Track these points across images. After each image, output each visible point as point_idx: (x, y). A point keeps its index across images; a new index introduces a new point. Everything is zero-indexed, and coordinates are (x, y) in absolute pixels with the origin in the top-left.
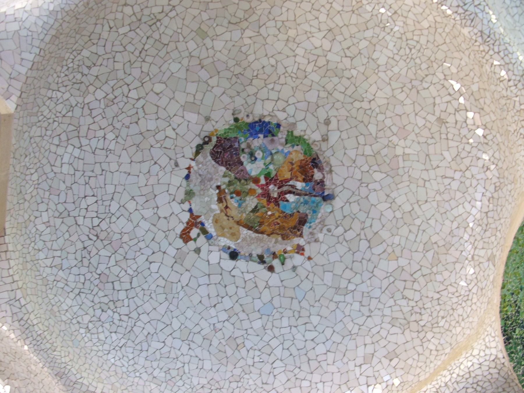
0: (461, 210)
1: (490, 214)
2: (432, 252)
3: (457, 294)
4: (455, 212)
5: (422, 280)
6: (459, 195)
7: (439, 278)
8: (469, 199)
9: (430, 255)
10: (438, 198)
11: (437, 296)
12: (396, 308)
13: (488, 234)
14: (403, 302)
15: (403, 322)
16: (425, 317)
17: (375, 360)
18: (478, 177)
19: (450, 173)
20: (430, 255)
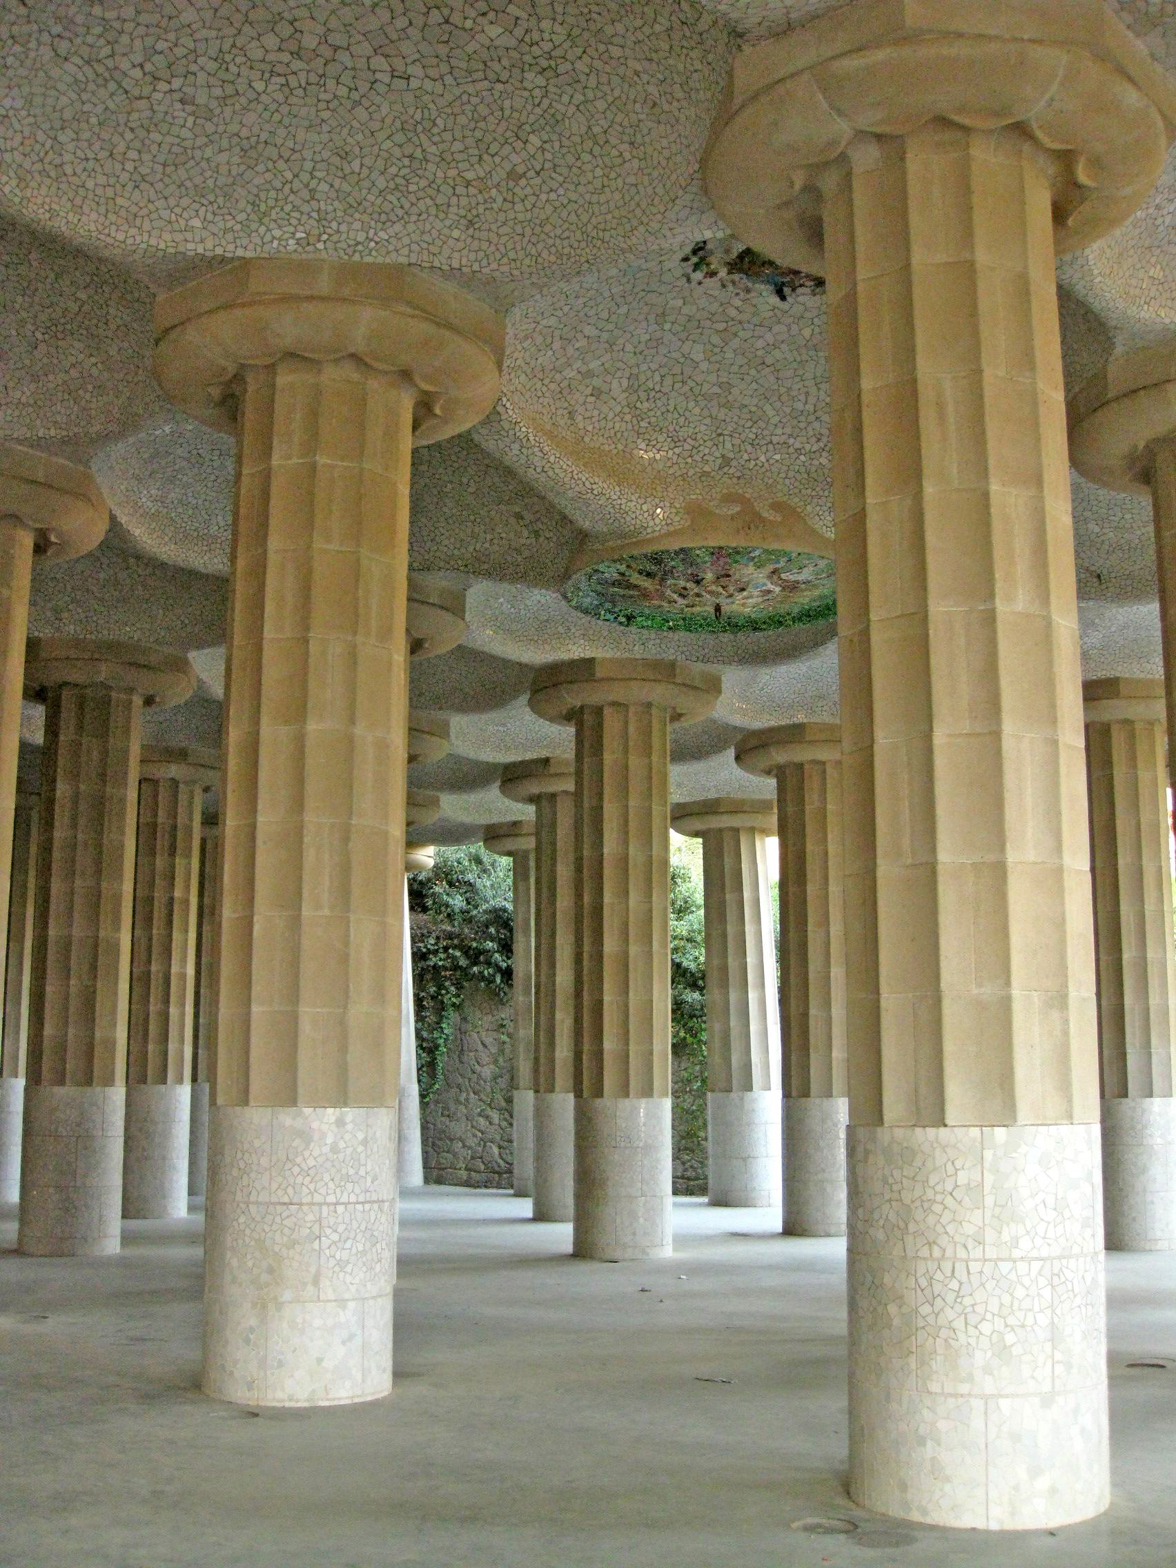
0: (771, 413)
1: (770, 447)
2: (719, 391)
3: (677, 428)
4: (767, 408)
5: (686, 388)
6: (788, 410)
7: (692, 404)
8: (784, 420)
9: (716, 390)
10: (783, 390)
11: (671, 408)
12: (649, 373)
13: (749, 448)
14: (657, 378)
15: (636, 386)
16: (646, 405)
17: (588, 381)
18: (810, 429)
19: (812, 400)
20: (716, 390)
